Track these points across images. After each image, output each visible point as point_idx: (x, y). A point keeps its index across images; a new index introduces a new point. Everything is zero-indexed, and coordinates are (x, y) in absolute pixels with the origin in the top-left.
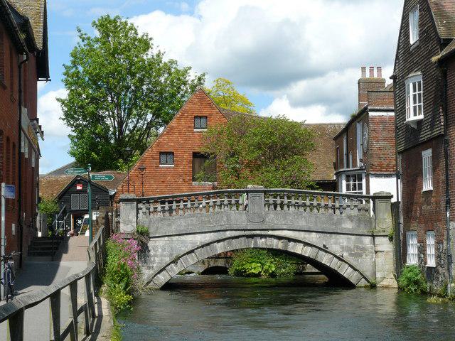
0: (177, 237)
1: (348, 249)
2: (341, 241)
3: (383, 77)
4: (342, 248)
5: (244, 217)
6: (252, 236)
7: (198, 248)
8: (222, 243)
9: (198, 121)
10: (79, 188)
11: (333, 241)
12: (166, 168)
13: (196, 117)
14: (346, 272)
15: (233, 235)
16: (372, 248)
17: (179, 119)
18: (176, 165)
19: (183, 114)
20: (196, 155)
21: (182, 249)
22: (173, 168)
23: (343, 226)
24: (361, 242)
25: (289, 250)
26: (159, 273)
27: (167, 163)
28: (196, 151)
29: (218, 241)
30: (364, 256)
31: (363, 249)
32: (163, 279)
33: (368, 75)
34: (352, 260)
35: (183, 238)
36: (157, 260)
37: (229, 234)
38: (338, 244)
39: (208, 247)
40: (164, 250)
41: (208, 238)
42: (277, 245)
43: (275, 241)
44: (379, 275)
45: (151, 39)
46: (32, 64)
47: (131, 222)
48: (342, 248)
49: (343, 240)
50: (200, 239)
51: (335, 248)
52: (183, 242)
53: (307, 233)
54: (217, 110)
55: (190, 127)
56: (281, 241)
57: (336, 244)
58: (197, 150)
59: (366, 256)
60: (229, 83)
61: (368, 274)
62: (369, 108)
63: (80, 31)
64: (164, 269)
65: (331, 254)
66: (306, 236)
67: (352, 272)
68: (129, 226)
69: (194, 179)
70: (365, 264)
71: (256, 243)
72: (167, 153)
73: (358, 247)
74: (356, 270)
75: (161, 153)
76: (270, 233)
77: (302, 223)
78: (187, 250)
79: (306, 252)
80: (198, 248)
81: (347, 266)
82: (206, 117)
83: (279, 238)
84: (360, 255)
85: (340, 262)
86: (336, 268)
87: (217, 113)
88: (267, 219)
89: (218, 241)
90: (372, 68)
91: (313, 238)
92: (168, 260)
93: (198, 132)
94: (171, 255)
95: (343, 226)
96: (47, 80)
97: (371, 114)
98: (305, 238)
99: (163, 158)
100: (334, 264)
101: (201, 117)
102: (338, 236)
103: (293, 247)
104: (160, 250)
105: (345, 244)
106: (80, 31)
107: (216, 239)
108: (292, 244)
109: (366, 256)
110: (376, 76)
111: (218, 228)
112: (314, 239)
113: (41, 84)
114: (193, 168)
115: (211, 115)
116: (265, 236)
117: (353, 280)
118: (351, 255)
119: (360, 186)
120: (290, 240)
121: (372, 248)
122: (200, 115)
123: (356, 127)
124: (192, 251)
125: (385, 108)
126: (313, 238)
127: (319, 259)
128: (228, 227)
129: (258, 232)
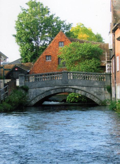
0: (38, 88)
2: (94, 90)
4: (94, 92)
6: (63, 88)
8: (53, 90)
9: (60, 43)
10: (16, 69)
12: (49, 62)
13: (59, 42)
14: (96, 100)
15: (57, 88)
16: (105, 92)
17: (53, 43)
19: (54, 41)
22: (51, 62)
23: (95, 84)
24: (101, 90)
29: (52, 90)
31: (102, 92)
34: (98, 96)
36: (31, 96)
37: (55, 87)
38: (93, 91)
40: (34, 93)
43: (71, 89)
48: (94, 92)
49: (95, 90)
50: (46, 89)
51: (92, 92)
52: (40, 90)
55: (57, 46)
56: (73, 89)
57: (92, 90)
60: (83, 25)
63: (21, 7)
65: (91, 94)
71: (65, 91)
72: (49, 56)
73: (100, 92)
75: (46, 56)
76: (69, 87)
77: (81, 83)
78: (41, 93)
80: (45, 92)
81: (96, 98)
82: (63, 42)
83: (73, 88)
85: (93, 97)
86: (92, 99)
87: (68, 40)
89: (52, 90)
91: (84, 88)
92: (35, 96)
94: (36, 95)
100: (91, 98)
101: (61, 42)
102: (93, 88)
103: (78, 92)
106: (21, 7)
107: (51, 89)
108: (77, 90)
115: (65, 41)
116: (68, 88)
118: (97, 94)
120: (76, 89)
121: (105, 92)
122: (61, 41)
124: (43, 93)
126: (84, 88)
127: (86, 96)
129: (65, 87)
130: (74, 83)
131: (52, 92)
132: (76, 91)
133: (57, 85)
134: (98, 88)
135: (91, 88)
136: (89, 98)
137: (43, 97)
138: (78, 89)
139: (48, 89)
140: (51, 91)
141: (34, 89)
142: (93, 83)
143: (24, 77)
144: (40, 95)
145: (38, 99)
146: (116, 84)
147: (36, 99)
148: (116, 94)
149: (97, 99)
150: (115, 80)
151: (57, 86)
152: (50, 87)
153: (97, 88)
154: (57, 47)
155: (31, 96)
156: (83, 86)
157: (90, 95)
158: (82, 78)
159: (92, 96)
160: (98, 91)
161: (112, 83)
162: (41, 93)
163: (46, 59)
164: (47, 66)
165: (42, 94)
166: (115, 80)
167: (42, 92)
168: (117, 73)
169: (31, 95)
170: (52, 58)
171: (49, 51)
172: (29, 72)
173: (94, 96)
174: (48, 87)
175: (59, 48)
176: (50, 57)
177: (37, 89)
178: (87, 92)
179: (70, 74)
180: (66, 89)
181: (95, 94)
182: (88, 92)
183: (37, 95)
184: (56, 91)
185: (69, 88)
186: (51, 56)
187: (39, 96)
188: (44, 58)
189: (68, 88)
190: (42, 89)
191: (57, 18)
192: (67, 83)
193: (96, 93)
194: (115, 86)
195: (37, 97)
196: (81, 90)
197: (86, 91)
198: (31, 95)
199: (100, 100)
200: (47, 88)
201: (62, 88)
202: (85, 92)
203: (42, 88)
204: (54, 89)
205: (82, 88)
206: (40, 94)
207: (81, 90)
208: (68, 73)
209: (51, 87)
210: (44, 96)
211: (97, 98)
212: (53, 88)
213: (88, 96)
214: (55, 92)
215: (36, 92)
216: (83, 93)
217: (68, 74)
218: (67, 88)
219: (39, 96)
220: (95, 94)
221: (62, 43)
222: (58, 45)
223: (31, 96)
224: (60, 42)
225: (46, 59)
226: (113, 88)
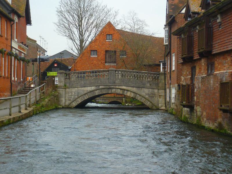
0: (80, 88)
1: (148, 94)
4: (146, 94)
6: (110, 88)
8: (98, 91)
9: (108, 36)
10: (56, 65)
13: (107, 34)
14: (148, 104)
16: (158, 94)
18: (98, 56)
20: (106, 51)
22: (96, 57)
26: (73, 102)
28: (107, 50)
32: (74, 104)
34: (150, 99)
35: (83, 89)
37: (101, 87)
40: (75, 93)
41: (93, 88)
42: (120, 92)
43: (119, 90)
44: (160, 105)
46: (23, 20)
47: (62, 82)
48: (146, 94)
49: (146, 91)
50: (89, 89)
51: (143, 94)
54: (117, 32)
55: (104, 39)
57: (144, 92)
58: (107, 49)
59: (156, 97)
61: (156, 104)
66: (132, 89)
69: (106, 63)
71: (111, 91)
72: (94, 50)
74: (151, 102)
76: (117, 87)
83: (121, 89)
84: (153, 97)
89: (96, 90)
91: (134, 89)
92: (76, 97)
93: (108, 41)
94: (78, 95)
96: (30, 25)
99: (92, 53)
100: (143, 100)
101: (109, 35)
102: (144, 89)
103: (126, 93)
108: (125, 92)
109: (156, 97)
111: (127, 86)
113: (28, 27)
115: (114, 34)
116: (115, 88)
120: (125, 90)
121: (158, 94)
129: (112, 87)
131: (97, 93)
132: (125, 93)
135: (143, 89)
137: (86, 99)
138: (128, 91)
140: (95, 91)
141: (76, 89)
143: (64, 74)
144: (82, 95)
145: (80, 101)
146: (171, 85)
148: (171, 97)
149: (149, 102)
150: (170, 79)
153: (149, 89)
155: (72, 97)
156: (133, 87)
157: (141, 97)
158: (132, 77)
159: (143, 98)
161: (166, 84)
162: (83, 93)
163: (91, 54)
165: (85, 94)
166: (170, 79)
167: (85, 92)
168: (172, 73)
169: (71, 95)
172: (70, 69)
174: (93, 87)
175: (106, 41)
178: (138, 94)
179: (118, 72)
183: (79, 95)
185: (117, 88)
187: (81, 96)
189: (115, 88)
190: (86, 89)
192: (115, 83)
193: (148, 95)
194: (170, 88)
195: (78, 98)
198: (71, 95)
200: (91, 87)
201: (108, 88)
205: (132, 89)
207: (131, 91)
208: (116, 71)
210: (88, 97)
211: (149, 101)
213: (138, 98)
214: (100, 93)
215: (78, 93)
217: (116, 72)
218: (114, 88)
219: (81, 96)
221: (110, 36)
222: (106, 38)
223: (72, 97)
224: (108, 34)
225: (91, 54)
226: (168, 90)
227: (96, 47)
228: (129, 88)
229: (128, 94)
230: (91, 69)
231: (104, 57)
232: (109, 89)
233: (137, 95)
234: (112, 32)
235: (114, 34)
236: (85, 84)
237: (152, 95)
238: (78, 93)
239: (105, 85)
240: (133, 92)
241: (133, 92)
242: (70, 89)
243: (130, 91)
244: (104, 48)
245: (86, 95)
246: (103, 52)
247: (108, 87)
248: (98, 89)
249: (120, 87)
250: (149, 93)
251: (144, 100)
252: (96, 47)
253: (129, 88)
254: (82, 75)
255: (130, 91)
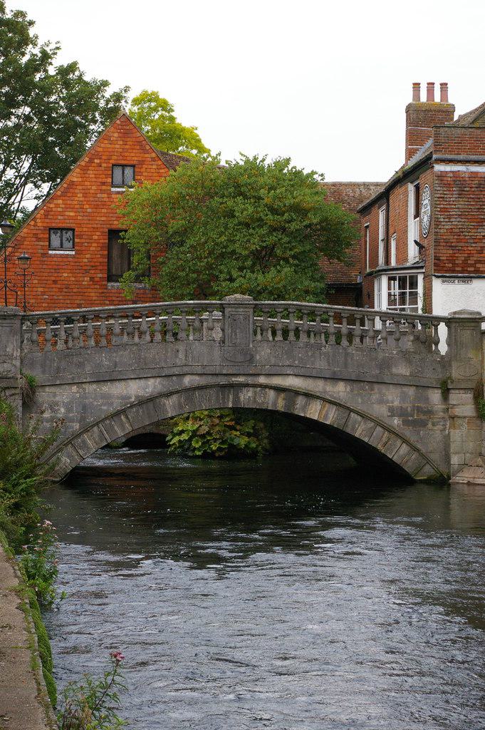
0: (94, 386)
1: (402, 413)
2: (390, 398)
3: (451, 101)
4: (391, 410)
5: (217, 353)
7: (131, 407)
8: (175, 397)
11: (375, 397)
14: (398, 453)
17: (85, 169)
21: (105, 408)
23: (394, 370)
25: (296, 412)
27: (61, 247)
28: (114, 227)
30: (430, 425)
31: (430, 412)
33: (423, 98)
34: (408, 432)
35: (106, 388)
37: (187, 381)
39: (151, 405)
40: (69, 410)
41: (151, 386)
42: (275, 404)
43: (272, 393)
44: (455, 460)
45: (31, 23)
47: (11, 357)
48: (391, 410)
49: (393, 397)
50: (135, 389)
51: (380, 411)
52: (106, 397)
53: (329, 383)
54: (154, 155)
55: (103, 184)
56: (283, 395)
57: (381, 402)
58: (117, 225)
61: (435, 457)
62: (434, 156)
64: (70, 442)
66: (328, 389)
67: (408, 453)
68: (5, 365)
69: (110, 278)
70: (432, 439)
71: (236, 398)
72: (62, 229)
73: (419, 410)
74: (416, 449)
75: (52, 230)
76: (262, 380)
77: (321, 364)
79: (326, 417)
80: (131, 407)
81: (399, 442)
82: (134, 166)
83: (279, 390)
84: (423, 424)
86: (379, 447)
87: (153, 160)
88: (258, 357)
90: (431, 85)
91: (340, 391)
92: (76, 426)
93: (118, 193)
94: (82, 419)
95: (394, 370)
97: (439, 168)
98: (325, 392)
99: (55, 240)
100: (376, 439)
101: (124, 166)
102: (383, 387)
103: (304, 408)
104: (63, 410)
105: (396, 403)
108: (300, 401)
109: (434, 425)
110: (437, 98)
112: (341, 394)
114: (109, 257)
115: (142, 163)
116: (254, 386)
117: (409, 468)
118: (406, 423)
119: (414, 296)
120: (297, 393)
122: (123, 162)
123: (406, 192)
124: (123, 411)
125: (461, 157)
127: (349, 430)
128: (186, 369)
129: (241, 379)
130: (288, 363)
133: (199, 370)
134: (411, 391)
135: (376, 386)
136: (366, 440)
138: (309, 396)
139: (150, 390)
140: (164, 400)
141: (74, 388)
142: (386, 365)
143: (18, 322)
144: (103, 420)
147: (84, 442)
149: (405, 448)
151: (197, 378)
152: (158, 380)
153: (405, 389)
154: (102, 191)
156: (334, 379)
159: (379, 429)
160: (408, 406)
162: (108, 409)
164: (53, 278)
165: (117, 414)
167: (117, 405)
170: (76, 240)
171: (68, 207)
173: (390, 431)
175: (110, 193)
176: (70, 233)
177: (91, 388)
180: (245, 390)
181: (396, 421)
182: (359, 408)
183: (91, 419)
184: (190, 400)
186: (73, 230)
187: (97, 424)
188: (39, 239)
189: (254, 386)
190: (117, 389)
191: (72, 67)
192: (251, 360)
193: (400, 416)
195: (86, 431)
196: (325, 400)
197: (348, 405)
199: (418, 450)
200: (142, 382)
202: (341, 409)
203: (117, 384)
204: (178, 392)
206: (106, 418)
207: (325, 400)
209: (165, 381)
210: (128, 428)
211: (405, 441)
212: (172, 385)
213: (360, 430)
215: (84, 407)
216: (331, 416)
218: (247, 385)
219: (97, 424)
220: (396, 422)
222: (110, 180)
227: (72, 214)
228: (317, 386)
229: (314, 411)
230: (53, 303)
231: (102, 256)
232: (227, 391)
233: (352, 414)
234: (134, 157)
235: (142, 163)
236: (116, 365)
237: (419, 418)
238: (84, 407)
239: (208, 370)
240: (331, 402)
241: (331, 402)
242: (47, 389)
243: (318, 398)
244: (103, 219)
245: (122, 417)
246: (100, 238)
247: (223, 380)
248: (178, 392)
249: (277, 381)
250: (404, 406)
251: (384, 439)
252: (72, 214)
253: (317, 386)
254: (62, 327)
255: (318, 398)
